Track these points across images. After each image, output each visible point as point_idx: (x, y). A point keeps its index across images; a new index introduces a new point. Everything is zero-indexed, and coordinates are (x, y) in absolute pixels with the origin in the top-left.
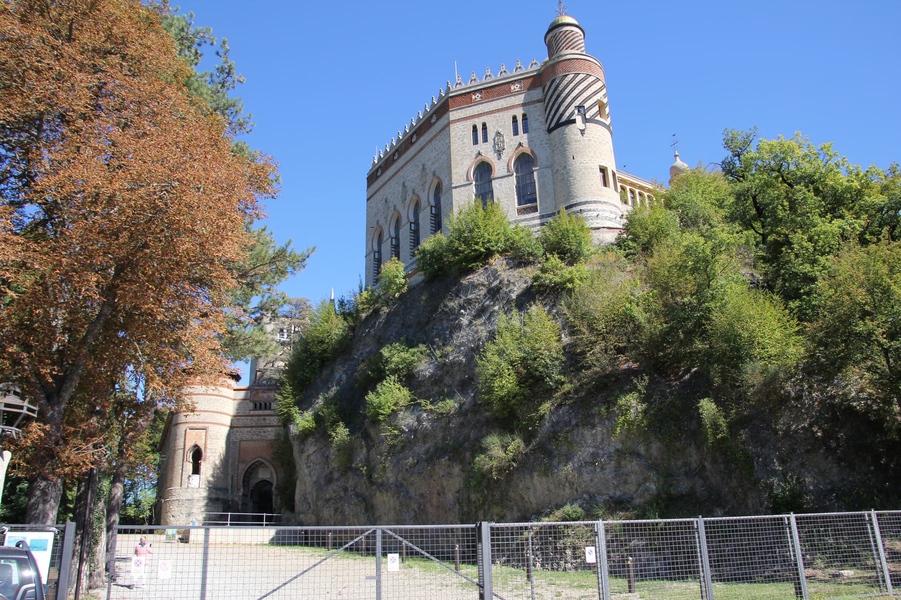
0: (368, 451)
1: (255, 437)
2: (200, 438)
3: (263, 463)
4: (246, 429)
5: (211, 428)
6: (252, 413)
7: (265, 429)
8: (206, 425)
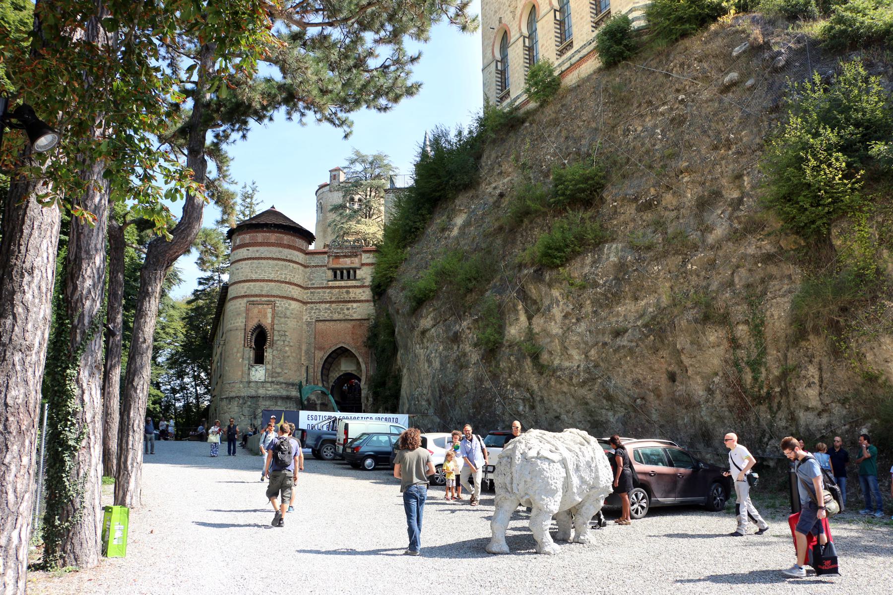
0: (530, 318)
1: (336, 316)
2: (265, 316)
3: (347, 350)
4: (323, 306)
5: (279, 302)
6: (331, 284)
7: (349, 305)
8: (273, 299)
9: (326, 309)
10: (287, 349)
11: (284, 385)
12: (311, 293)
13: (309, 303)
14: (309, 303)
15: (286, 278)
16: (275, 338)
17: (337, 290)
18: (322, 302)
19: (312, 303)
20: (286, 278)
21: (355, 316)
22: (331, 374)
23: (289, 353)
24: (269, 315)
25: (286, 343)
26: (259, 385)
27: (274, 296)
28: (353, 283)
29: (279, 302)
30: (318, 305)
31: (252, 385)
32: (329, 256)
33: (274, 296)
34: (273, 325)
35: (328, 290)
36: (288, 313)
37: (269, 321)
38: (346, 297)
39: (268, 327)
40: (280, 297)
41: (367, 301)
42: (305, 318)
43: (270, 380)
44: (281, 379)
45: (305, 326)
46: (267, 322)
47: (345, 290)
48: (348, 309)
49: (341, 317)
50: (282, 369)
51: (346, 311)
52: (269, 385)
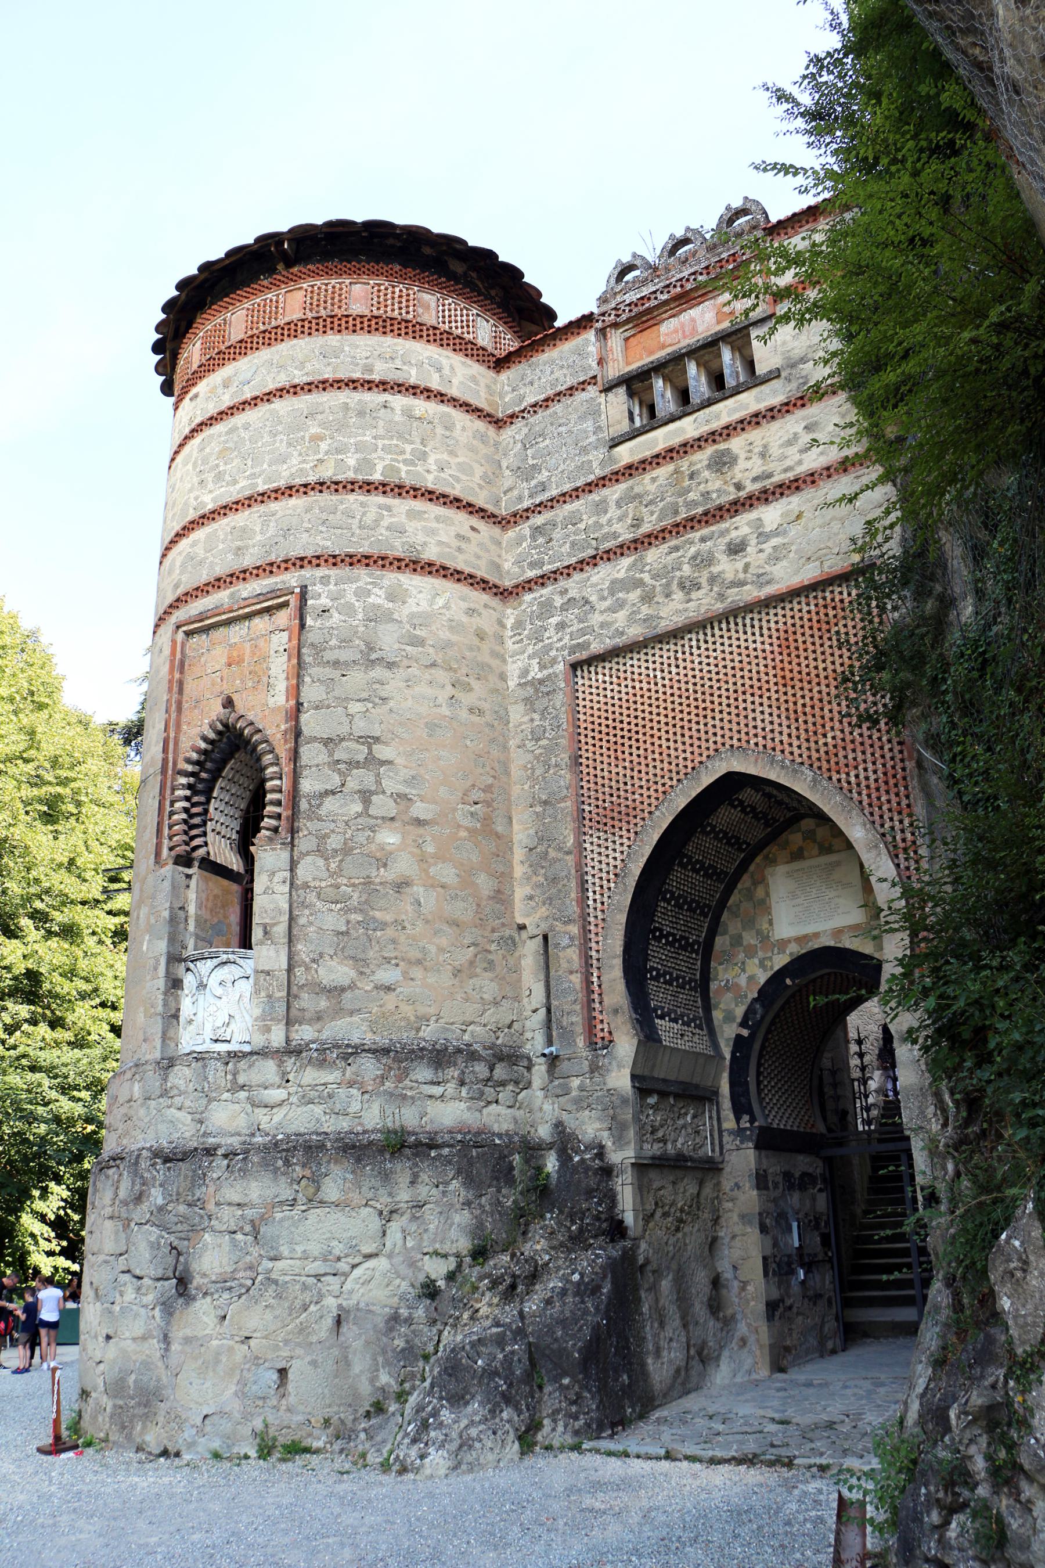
4: (602, 575)
5: (325, 588)
6: (626, 454)
7: (741, 525)
8: (292, 579)
9: (616, 586)
10: (389, 838)
11: (369, 1067)
12: (537, 530)
13: (528, 585)
14: (528, 585)
15: (366, 464)
17: (664, 472)
18: (593, 561)
19: (542, 580)
20: (366, 464)
21: (787, 575)
22: (723, 975)
23: (403, 866)
24: (279, 667)
25: (382, 806)
26: (216, 1073)
27: (301, 562)
28: (749, 402)
29: (325, 588)
30: (573, 585)
31: (181, 1076)
32: (602, 333)
33: (301, 562)
35: (614, 492)
36: (388, 640)
37: (279, 698)
38: (718, 489)
39: (274, 729)
40: (334, 560)
41: (845, 466)
42: (513, 669)
44: (353, 1029)
45: (517, 714)
46: (264, 710)
47: (701, 458)
48: (736, 549)
49: (705, 602)
50: (360, 963)
51: (727, 567)
52: (269, 1069)
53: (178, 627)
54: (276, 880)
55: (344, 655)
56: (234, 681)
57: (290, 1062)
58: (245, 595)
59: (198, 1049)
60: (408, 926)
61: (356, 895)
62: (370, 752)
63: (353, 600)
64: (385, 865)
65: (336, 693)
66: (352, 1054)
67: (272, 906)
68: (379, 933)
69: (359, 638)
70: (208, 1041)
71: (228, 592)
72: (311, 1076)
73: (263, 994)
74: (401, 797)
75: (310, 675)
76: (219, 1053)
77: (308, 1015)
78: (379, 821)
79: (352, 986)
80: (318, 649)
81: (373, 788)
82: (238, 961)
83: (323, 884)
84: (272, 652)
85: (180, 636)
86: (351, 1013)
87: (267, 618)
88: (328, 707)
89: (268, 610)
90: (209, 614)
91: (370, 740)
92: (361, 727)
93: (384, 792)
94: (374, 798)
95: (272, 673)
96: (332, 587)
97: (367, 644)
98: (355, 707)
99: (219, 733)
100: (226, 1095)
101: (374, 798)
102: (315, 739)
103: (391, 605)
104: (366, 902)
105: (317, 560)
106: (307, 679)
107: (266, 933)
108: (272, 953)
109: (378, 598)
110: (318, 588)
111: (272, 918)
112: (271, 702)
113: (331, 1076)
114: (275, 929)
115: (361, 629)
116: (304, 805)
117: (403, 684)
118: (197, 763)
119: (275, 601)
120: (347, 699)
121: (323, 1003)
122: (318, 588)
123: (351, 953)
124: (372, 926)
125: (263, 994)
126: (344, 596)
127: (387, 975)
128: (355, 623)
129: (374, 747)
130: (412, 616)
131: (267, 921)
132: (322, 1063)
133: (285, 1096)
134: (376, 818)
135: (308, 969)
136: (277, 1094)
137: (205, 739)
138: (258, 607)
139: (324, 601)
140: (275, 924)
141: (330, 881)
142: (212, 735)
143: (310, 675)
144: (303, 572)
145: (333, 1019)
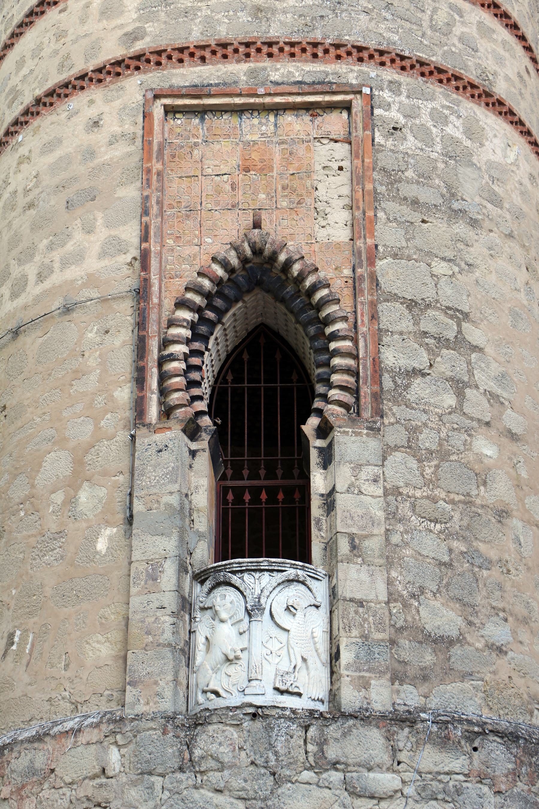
8: (349, 72)
10: (486, 448)
16: (390, 357)
23: (500, 490)
24: (333, 189)
25: (477, 404)
26: (289, 741)
27: (360, 53)
29: (397, 98)
33: (360, 53)
34: (365, 258)
36: (470, 189)
37: (336, 228)
39: (332, 273)
40: (402, 62)
43: (381, 696)
44: (462, 698)
50: (467, 607)
52: (370, 743)
53: (156, 97)
54: (363, 475)
55: (426, 195)
56: (255, 193)
57: (403, 735)
58: (275, 76)
59: (258, 701)
60: (513, 571)
61: (457, 516)
62: (460, 332)
63: (430, 124)
64: (485, 483)
65: (418, 242)
66: (478, 734)
67: (360, 512)
68: (485, 573)
69: (438, 176)
70: (270, 691)
71: (244, 67)
72: (430, 758)
73: (355, 632)
74: (493, 397)
75: (384, 210)
76: (294, 711)
77: (411, 671)
78: (475, 424)
79: (460, 640)
80: (393, 178)
81: (466, 379)
82: (309, 581)
83: (418, 493)
84: (318, 167)
85: (158, 111)
86: (465, 676)
87: (307, 118)
88: (409, 258)
89: (308, 107)
90: (213, 90)
91: (461, 316)
92: (447, 294)
93: (477, 387)
94: (468, 391)
95: (321, 193)
96: (403, 98)
97: (449, 187)
98: (441, 268)
99: (244, 260)
100: (307, 775)
101: (468, 391)
102: (395, 297)
103: (468, 143)
104: (468, 528)
105: (381, 56)
106: (381, 215)
107: (354, 547)
108: (364, 576)
109: (455, 129)
110: (386, 95)
111: (364, 528)
112: (321, 234)
113: (457, 763)
114: (366, 543)
115: (441, 165)
116: (387, 383)
117: (486, 252)
118: (208, 296)
119: (327, 98)
120: (429, 253)
121: (429, 658)
122: (386, 95)
123: (458, 593)
124: (477, 561)
125: (355, 632)
126: (418, 116)
127: (497, 632)
128: (434, 155)
129: (463, 323)
130: (490, 164)
131: (354, 530)
132: (444, 742)
133: (397, 784)
134: (472, 419)
135: (406, 606)
136: (386, 781)
137: (225, 264)
138: (299, 99)
139: (395, 115)
140: (366, 537)
141: (426, 492)
142: (234, 261)
143: (384, 210)
144: (364, 68)
145: (442, 681)
